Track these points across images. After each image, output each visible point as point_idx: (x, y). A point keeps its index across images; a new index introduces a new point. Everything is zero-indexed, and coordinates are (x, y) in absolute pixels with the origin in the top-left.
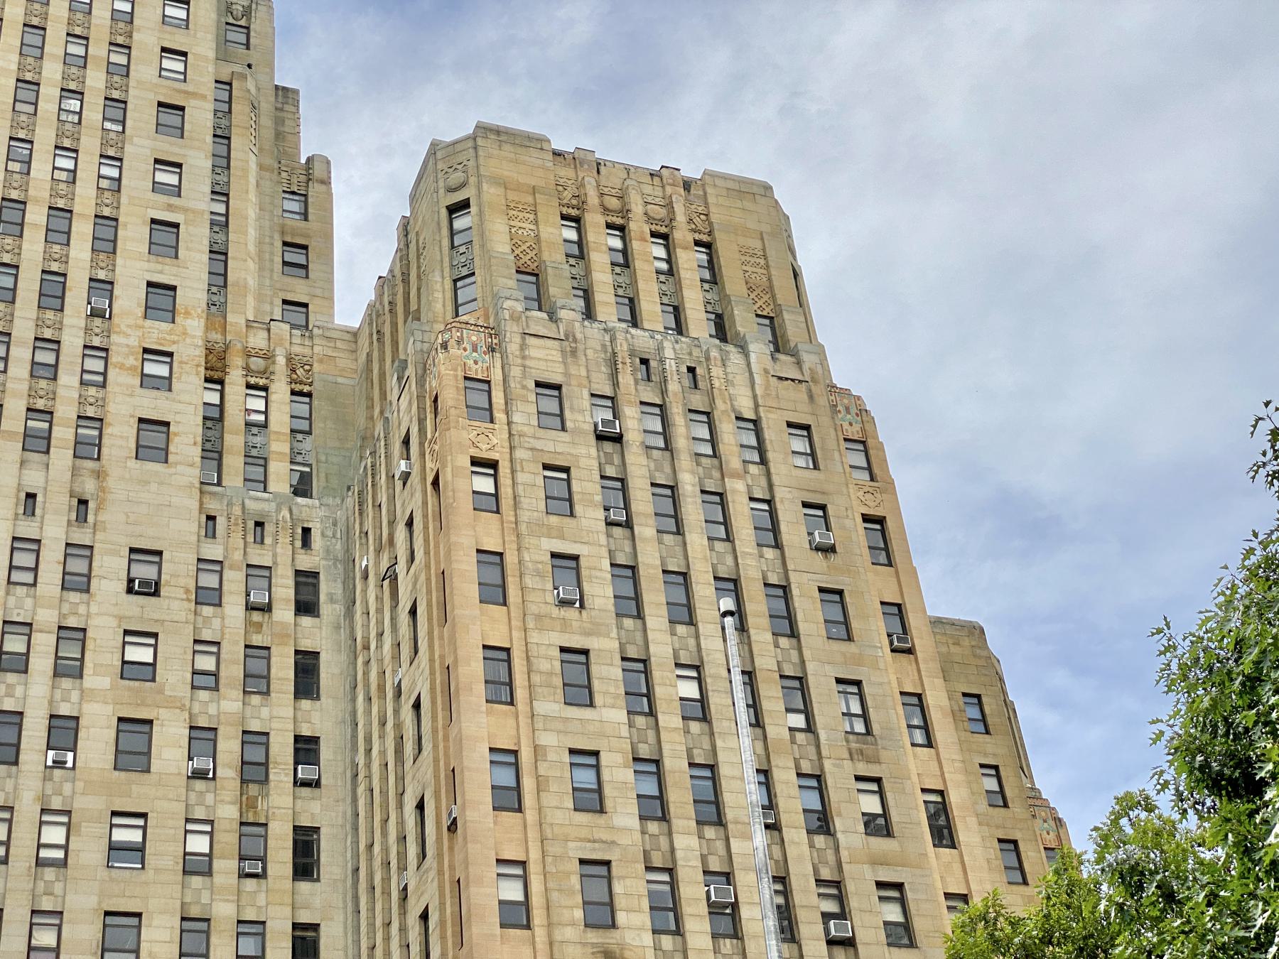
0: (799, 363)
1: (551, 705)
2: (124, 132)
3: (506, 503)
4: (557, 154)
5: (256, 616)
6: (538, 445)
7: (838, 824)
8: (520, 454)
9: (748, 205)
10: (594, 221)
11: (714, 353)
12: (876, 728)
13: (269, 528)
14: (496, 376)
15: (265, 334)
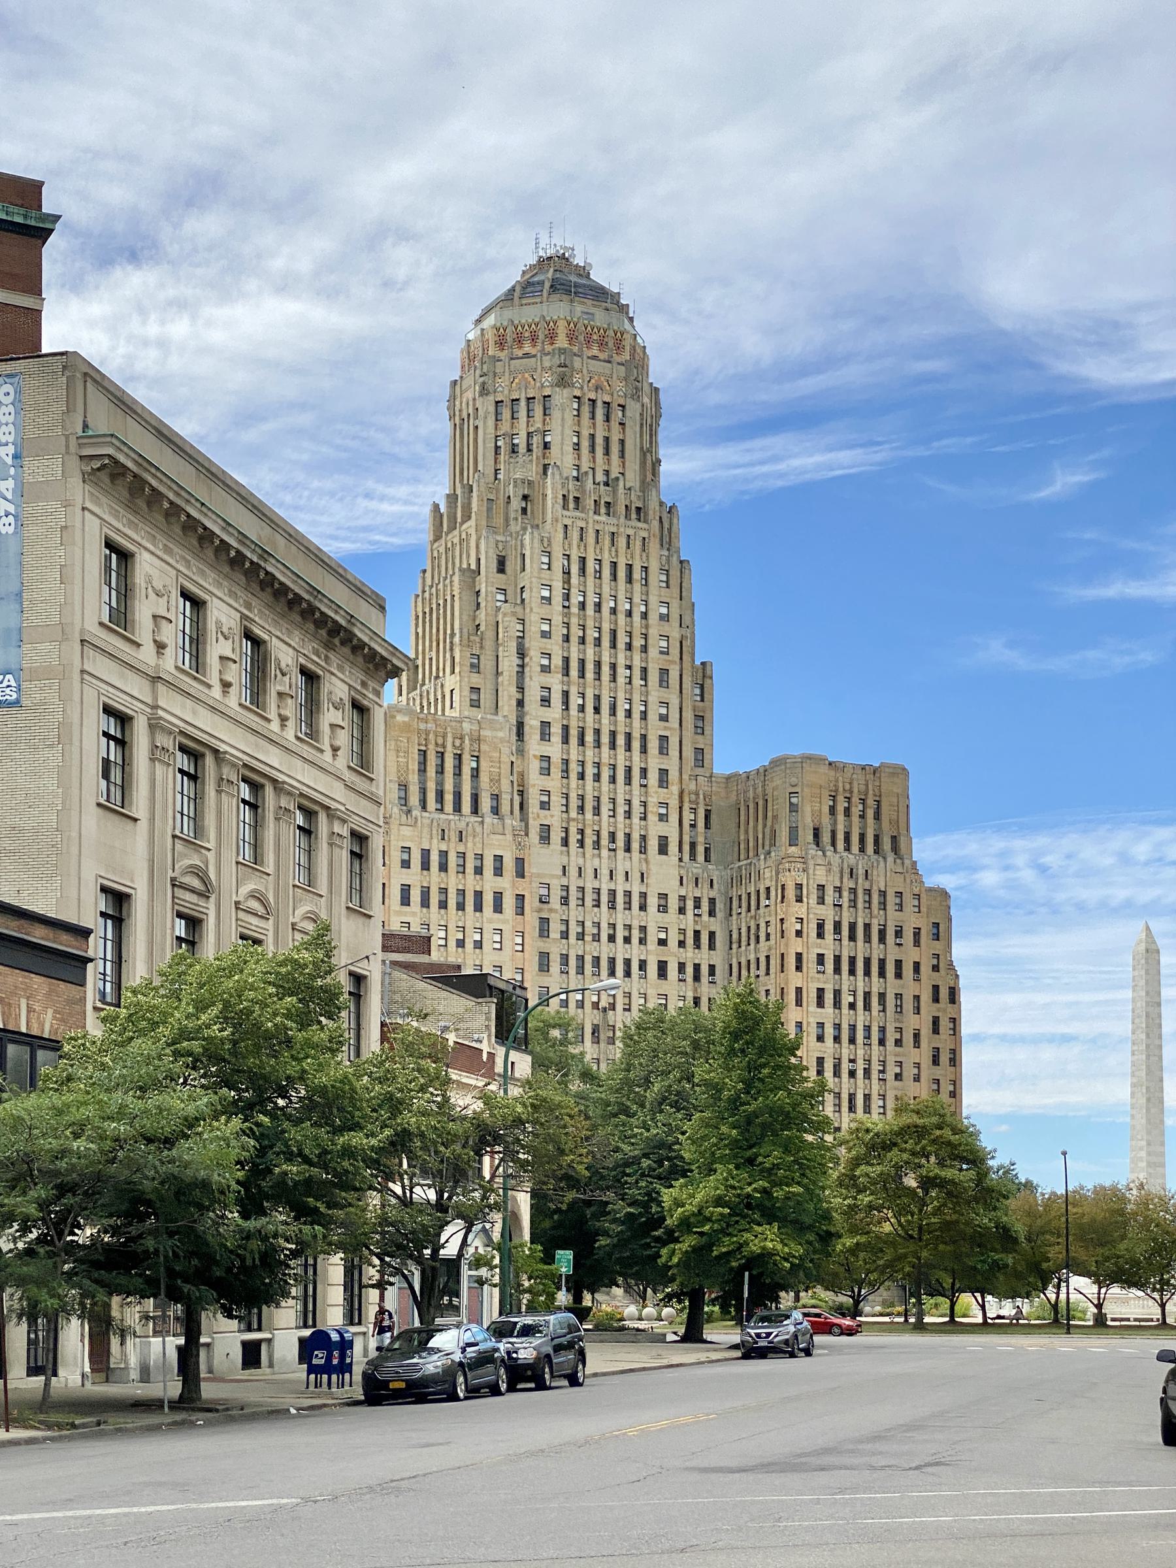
0: (903, 863)
1: (813, 1008)
2: (646, 685)
3: (805, 935)
4: (830, 764)
5: (697, 918)
6: (817, 911)
7: (888, 1044)
8: (811, 916)
9: (896, 780)
10: (840, 798)
11: (875, 864)
12: (904, 1011)
13: (700, 880)
14: (805, 883)
15: (694, 782)
